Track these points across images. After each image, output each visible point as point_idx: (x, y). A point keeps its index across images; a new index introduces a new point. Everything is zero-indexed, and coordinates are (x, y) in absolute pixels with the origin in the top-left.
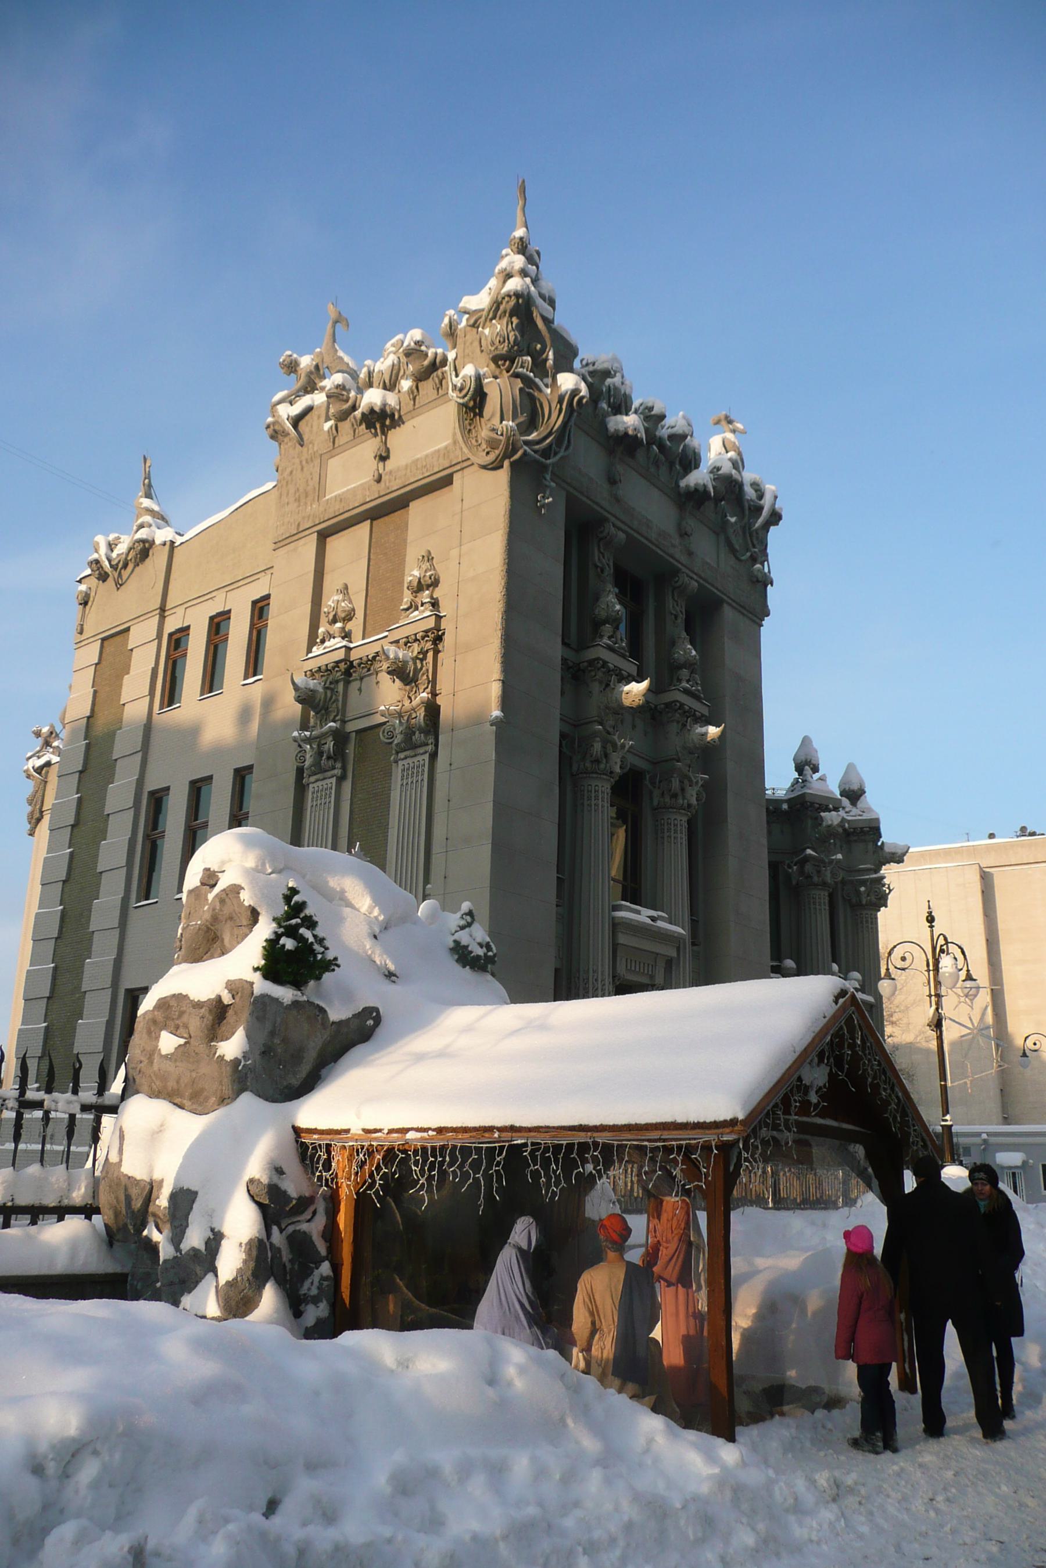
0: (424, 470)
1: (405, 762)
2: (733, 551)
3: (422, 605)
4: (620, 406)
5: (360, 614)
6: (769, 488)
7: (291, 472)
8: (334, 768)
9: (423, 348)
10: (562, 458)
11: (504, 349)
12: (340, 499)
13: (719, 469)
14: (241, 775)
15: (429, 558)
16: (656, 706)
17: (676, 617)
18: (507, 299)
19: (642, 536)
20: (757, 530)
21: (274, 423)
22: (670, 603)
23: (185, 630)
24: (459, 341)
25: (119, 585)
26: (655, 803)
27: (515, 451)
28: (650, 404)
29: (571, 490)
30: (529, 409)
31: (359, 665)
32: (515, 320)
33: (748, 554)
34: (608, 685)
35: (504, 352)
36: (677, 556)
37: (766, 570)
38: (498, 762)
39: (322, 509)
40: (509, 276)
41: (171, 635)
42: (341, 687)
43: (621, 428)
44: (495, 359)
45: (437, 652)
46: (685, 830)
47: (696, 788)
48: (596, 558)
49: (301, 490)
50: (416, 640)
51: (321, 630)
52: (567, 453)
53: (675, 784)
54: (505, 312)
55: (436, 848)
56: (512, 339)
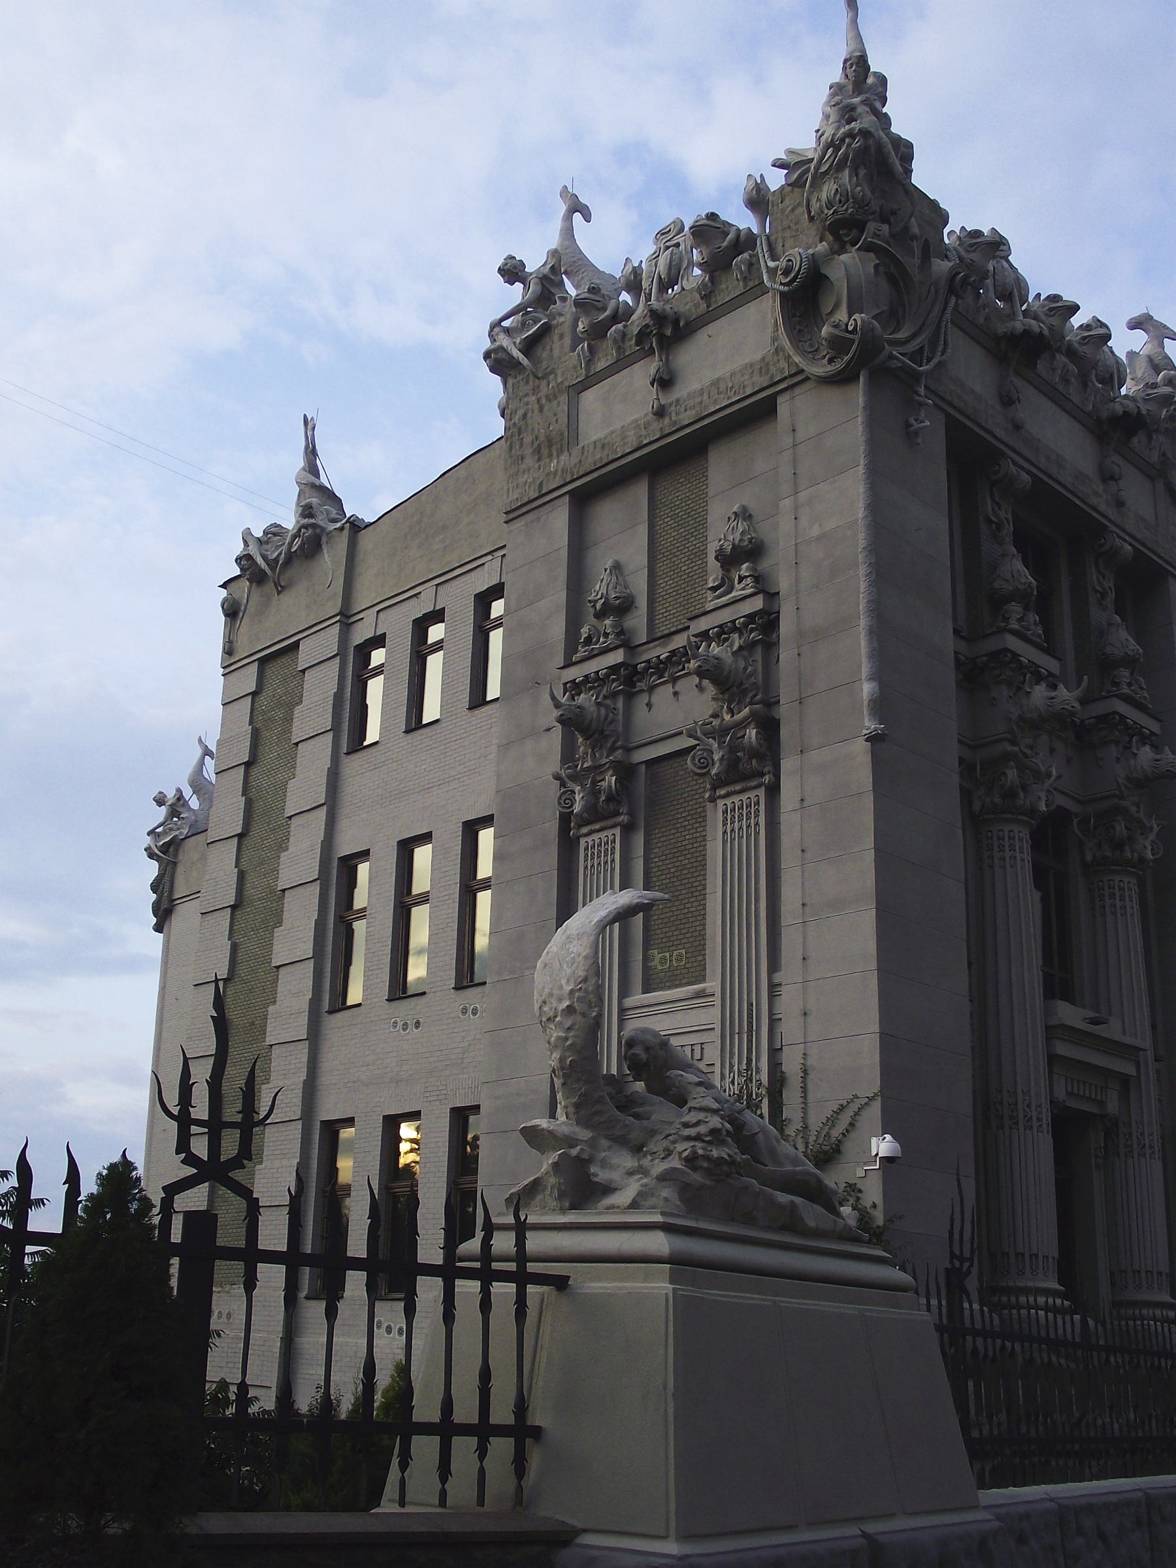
3: (741, 579)
5: (642, 603)
18: (847, 140)
31: (646, 669)
42: (620, 704)
49: (542, 438)
50: (735, 629)
51: (585, 631)
54: (846, 156)
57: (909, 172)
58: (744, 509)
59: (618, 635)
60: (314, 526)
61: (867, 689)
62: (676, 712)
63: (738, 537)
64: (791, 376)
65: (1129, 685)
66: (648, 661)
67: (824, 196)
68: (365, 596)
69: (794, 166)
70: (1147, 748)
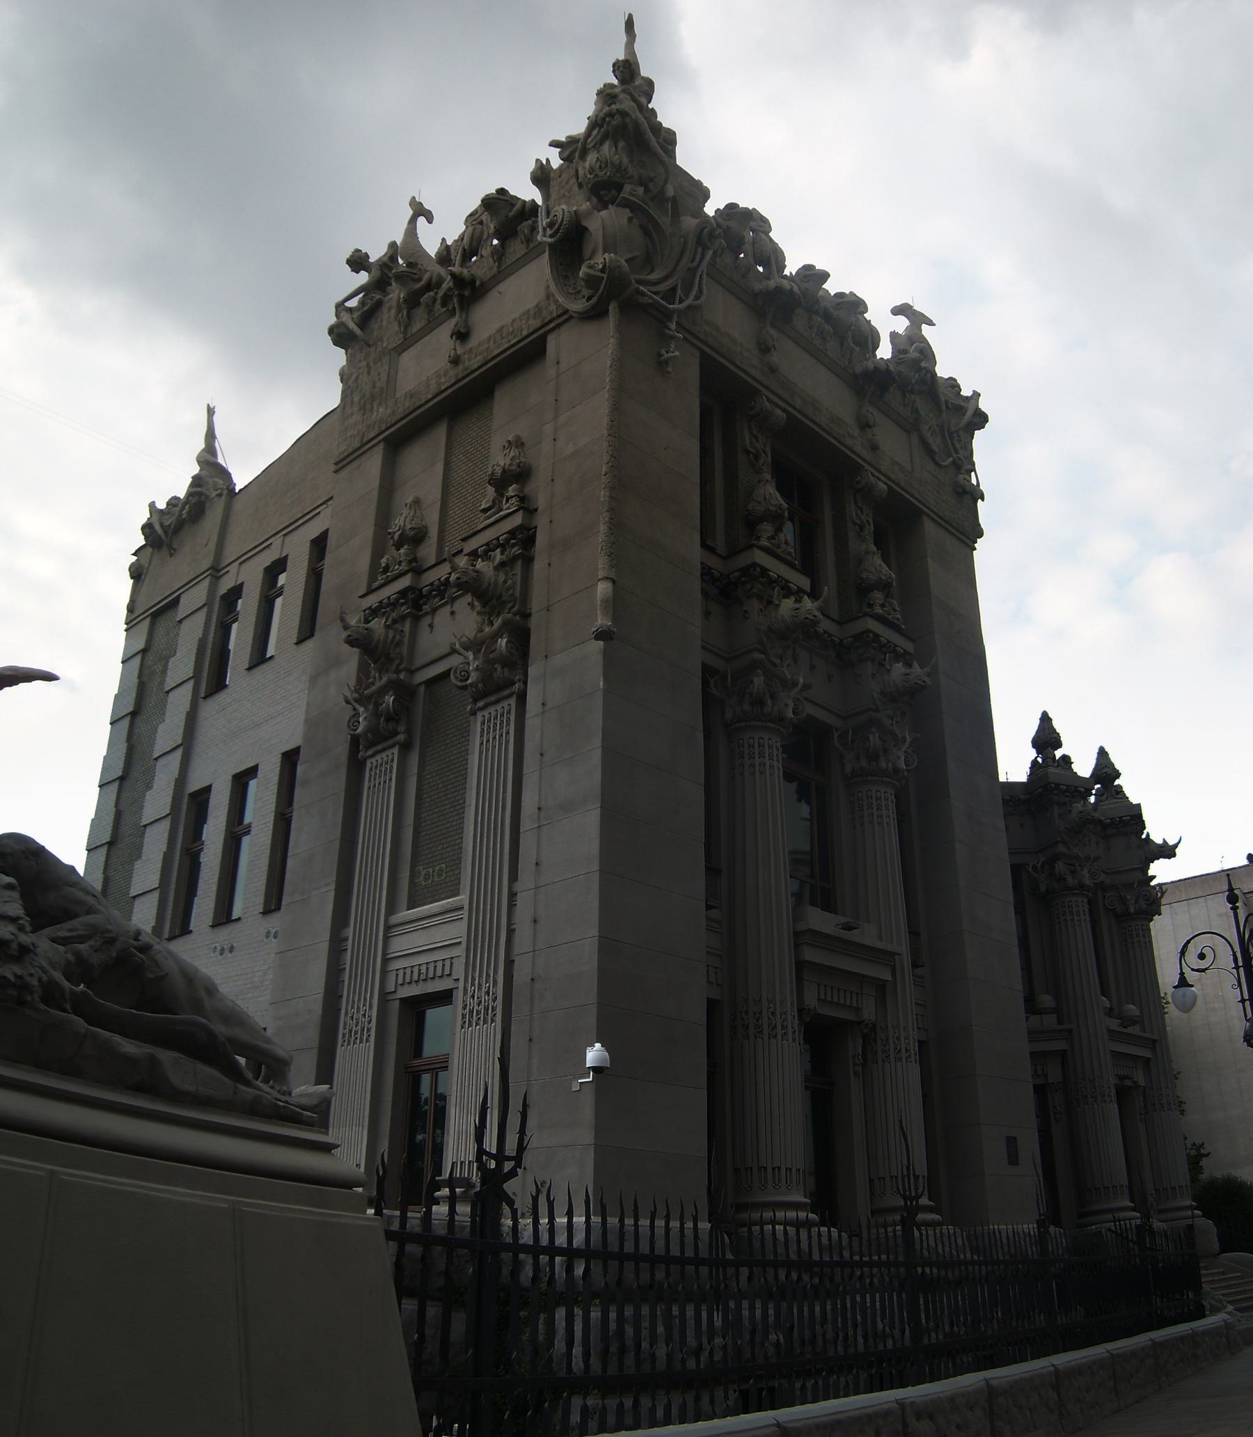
1: (486, 713)
2: (930, 453)
4: (769, 258)
5: (434, 533)
7: (357, 378)
8: (396, 733)
10: (689, 307)
11: (605, 174)
14: (290, 759)
16: (841, 641)
17: (862, 528)
23: (236, 592)
25: (172, 551)
26: (848, 769)
31: (430, 592)
33: (951, 459)
34: (770, 602)
36: (858, 449)
37: (974, 481)
38: (606, 692)
41: (223, 597)
42: (407, 627)
45: (528, 560)
46: (892, 806)
47: (904, 749)
52: (698, 302)
53: (874, 739)
55: (526, 824)
57: (672, 154)
58: (518, 438)
59: (410, 562)
60: (200, 494)
61: (603, 589)
62: (452, 630)
63: (508, 462)
64: (558, 316)
65: (883, 606)
66: (432, 584)
67: (587, 165)
68: (231, 552)
69: (570, 148)
70: (900, 665)
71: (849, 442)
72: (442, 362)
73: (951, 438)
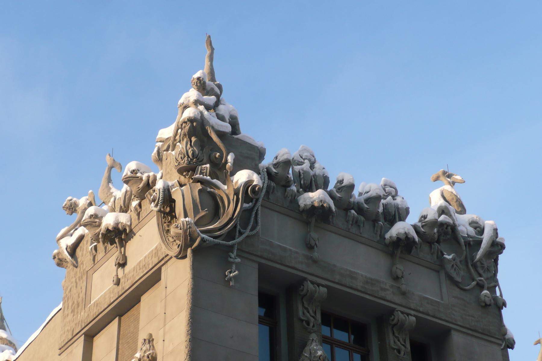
0: (144, 269)
6: (488, 224)
9: (139, 175)
10: (248, 237)
11: (184, 163)
12: (97, 304)
13: (425, 217)
15: (150, 340)
17: (399, 351)
18: (184, 125)
19: (345, 286)
20: (480, 260)
21: (58, 254)
22: (391, 340)
24: (164, 162)
27: (193, 241)
28: (340, 179)
29: (263, 261)
30: (211, 203)
32: (193, 139)
33: (474, 283)
35: (185, 165)
36: (389, 297)
37: (498, 294)
39: (86, 315)
40: (186, 107)
43: (308, 202)
44: (181, 171)
48: (301, 313)
52: (255, 232)
56: (190, 154)
71: (382, 294)
72: (110, 284)
73: (475, 266)
